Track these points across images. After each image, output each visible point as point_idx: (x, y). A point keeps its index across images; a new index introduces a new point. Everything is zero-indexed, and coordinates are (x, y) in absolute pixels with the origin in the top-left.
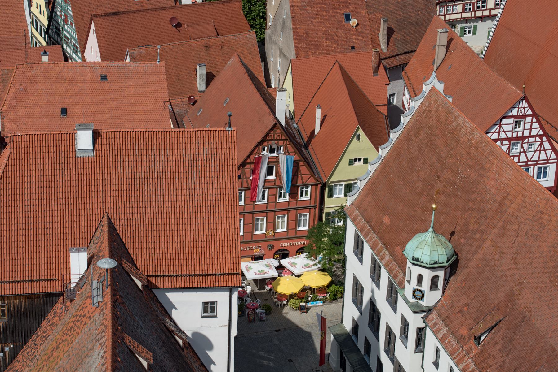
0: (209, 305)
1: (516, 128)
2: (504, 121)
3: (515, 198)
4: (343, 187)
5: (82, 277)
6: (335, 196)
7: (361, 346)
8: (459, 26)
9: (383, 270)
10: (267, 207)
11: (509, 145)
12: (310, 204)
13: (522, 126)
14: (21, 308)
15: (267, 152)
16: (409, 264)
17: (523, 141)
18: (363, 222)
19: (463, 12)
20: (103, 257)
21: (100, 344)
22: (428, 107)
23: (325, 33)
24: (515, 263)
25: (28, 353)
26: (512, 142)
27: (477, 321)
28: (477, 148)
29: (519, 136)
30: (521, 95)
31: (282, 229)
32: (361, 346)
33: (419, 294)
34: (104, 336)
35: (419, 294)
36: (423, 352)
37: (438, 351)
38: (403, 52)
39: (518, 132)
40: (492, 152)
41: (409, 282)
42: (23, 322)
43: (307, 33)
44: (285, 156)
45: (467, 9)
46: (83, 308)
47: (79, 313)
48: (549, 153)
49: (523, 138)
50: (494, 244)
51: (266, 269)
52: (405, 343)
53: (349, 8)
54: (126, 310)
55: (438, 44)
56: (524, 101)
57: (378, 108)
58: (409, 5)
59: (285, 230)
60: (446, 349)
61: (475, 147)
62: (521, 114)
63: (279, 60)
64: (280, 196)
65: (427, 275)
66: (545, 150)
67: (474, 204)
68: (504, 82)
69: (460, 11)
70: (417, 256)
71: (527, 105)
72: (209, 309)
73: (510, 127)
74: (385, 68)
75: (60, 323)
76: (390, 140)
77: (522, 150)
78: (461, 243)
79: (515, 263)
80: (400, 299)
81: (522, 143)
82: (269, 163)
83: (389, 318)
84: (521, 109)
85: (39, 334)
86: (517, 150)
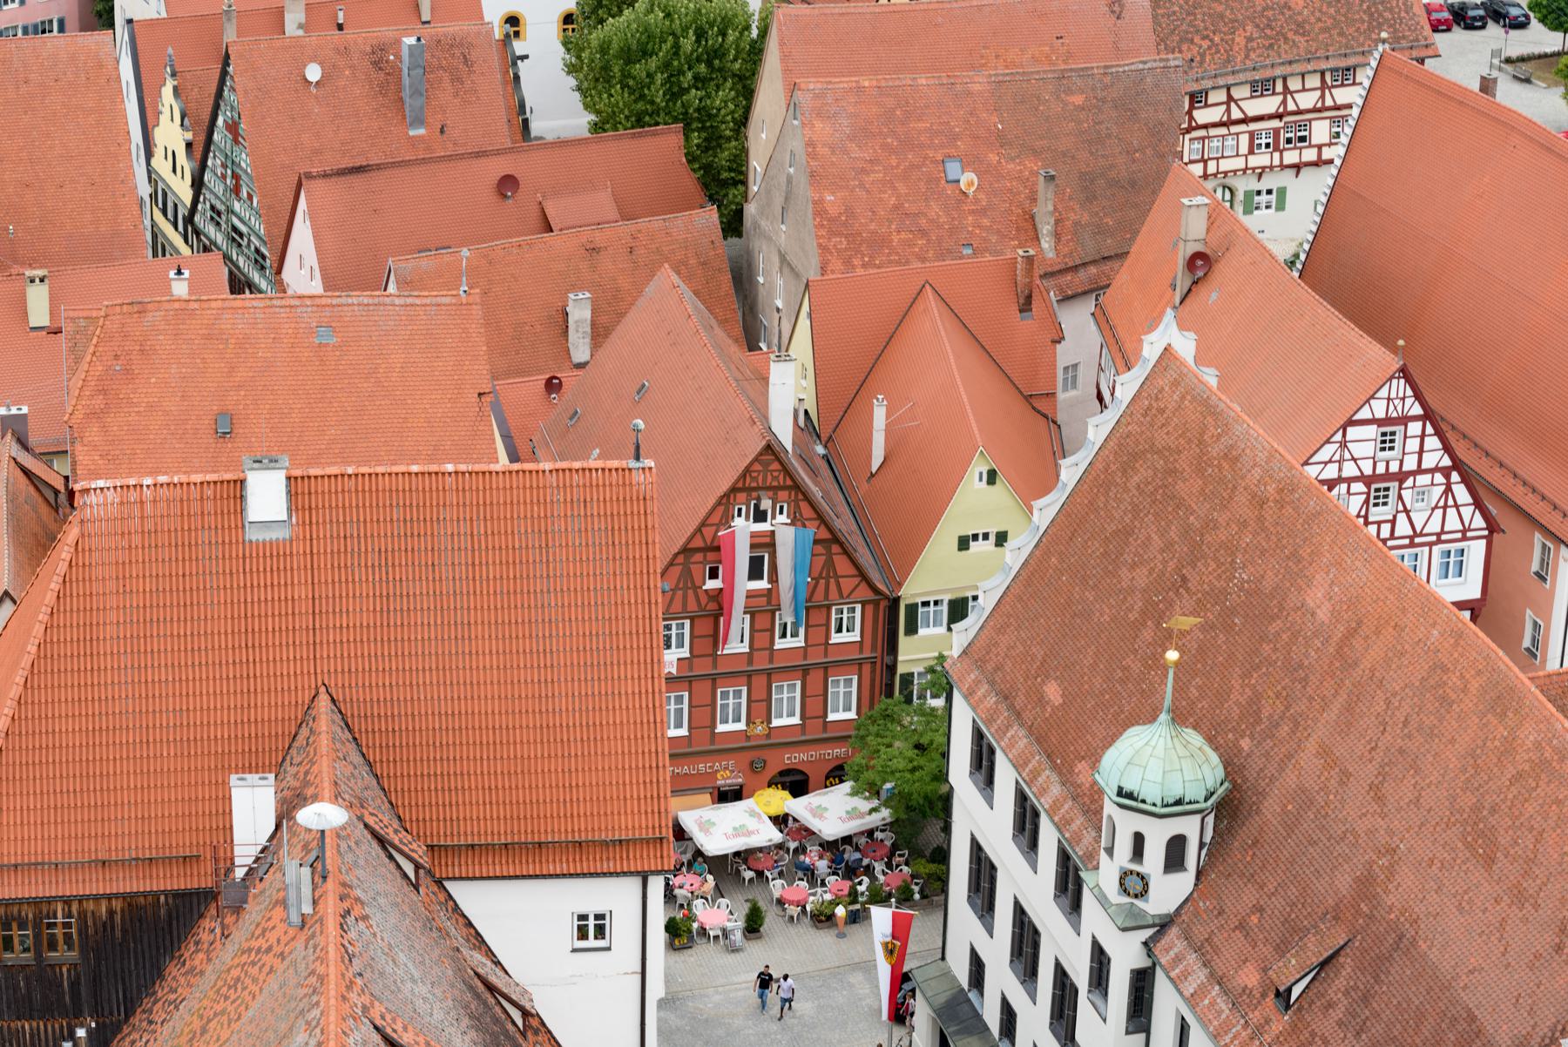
0: (591, 923)
1: (1383, 449)
2: (1353, 432)
3: (1378, 633)
4: (945, 608)
5: (262, 851)
6: (922, 631)
7: (992, 1017)
9: (1044, 822)
10: (750, 662)
11: (1368, 494)
12: (861, 651)
14: (113, 928)
15: (747, 518)
16: (1109, 809)
17: (1401, 482)
18: (992, 700)
19: (1251, 152)
20: (315, 798)
21: (308, 1023)
23: (896, 207)
24: (1379, 799)
25: (133, 1042)
26: (1374, 487)
27: (1282, 949)
28: (1281, 504)
31: (786, 720)
32: (992, 1017)
33: (1134, 884)
34: (317, 1004)
35: (1134, 884)
36: (1146, 1030)
37: (1184, 1029)
41: (1110, 851)
42: (118, 965)
43: (850, 212)
44: (792, 529)
46: (264, 931)
47: (255, 944)
48: (1467, 512)
49: (1401, 477)
50: (1324, 751)
51: (752, 824)
52: (1102, 1010)
53: (957, 147)
54: (375, 935)
58: (1109, 136)
59: (796, 720)
60: (1204, 1024)
63: (780, 282)
64: (784, 635)
65: (1157, 837)
66: (1456, 506)
67: (1275, 650)
69: (1244, 149)
70: (1128, 786)
71: (1409, 392)
72: (592, 928)
75: (210, 968)
77: (1401, 507)
78: (1240, 750)
79: (1379, 799)
80: (1088, 899)
81: (1400, 488)
82: (753, 546)
83: (1064, 947)
85: (160, 994)
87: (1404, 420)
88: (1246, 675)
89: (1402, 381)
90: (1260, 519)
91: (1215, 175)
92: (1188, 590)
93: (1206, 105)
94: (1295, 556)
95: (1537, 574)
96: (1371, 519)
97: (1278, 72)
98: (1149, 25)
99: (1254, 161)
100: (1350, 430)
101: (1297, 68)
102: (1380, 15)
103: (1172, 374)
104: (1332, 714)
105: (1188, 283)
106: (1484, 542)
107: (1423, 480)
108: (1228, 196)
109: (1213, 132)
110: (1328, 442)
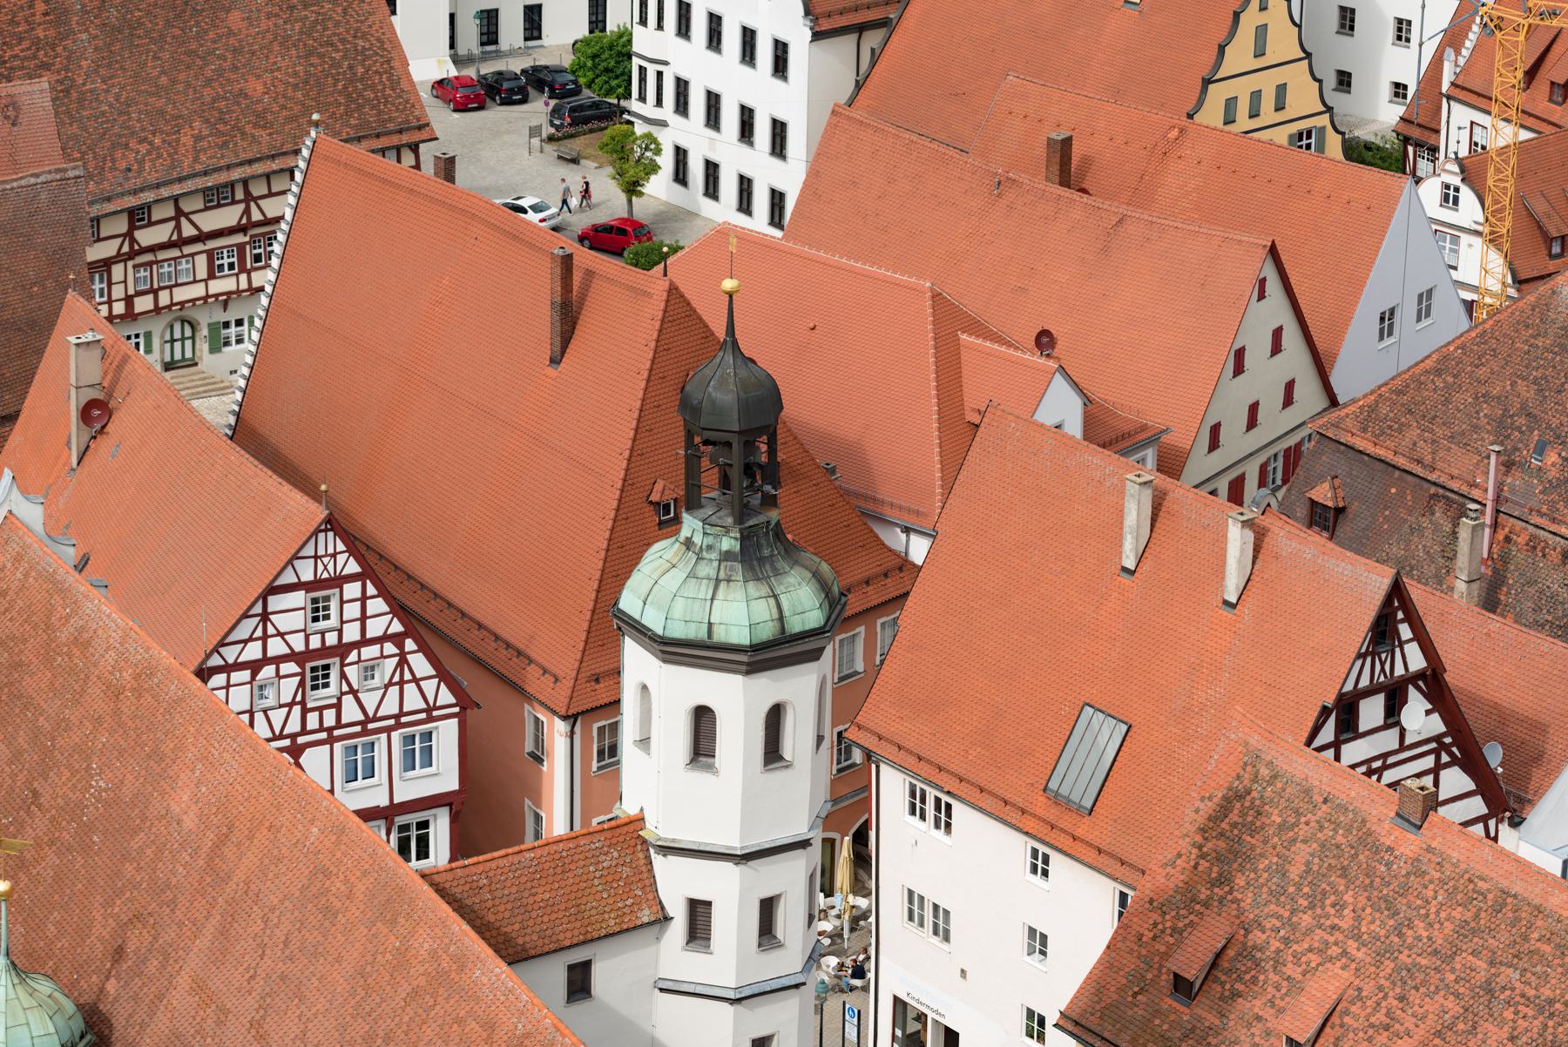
1: (316, 619)
2: (275, 602)
3: (251, 838)
11: (302, 674)
17: (343, 657)
19: (211, 276)
26: (309, 665)
28: (138, 692)
29: (312, 647)
30: (321, 513)
39: (323, 633)
45: (221, 267)
48: (429, 687)
49: (342, 650)
50: (199, 987)
61: (133, 690)
62: (325, 575)
66: (416, 680)
69: (202, 272)
71: (341, 547)
73: (296, 620)
77: (345, 688)
81: (343, 665)
84: (326, 560)
87: (339, 581)
88: (109, 903)
89: (331, 534)
90: (117, 712)
91: (169, 307)
92: (39, 807)
93: (151, 224)
95: (531, 754)
97: (236, 174)
98: (52, 129)
99: (217, 286)
100: (271, 599)
101: (259, 168)
102: (360, 95)
104: (203, 942)
105: (86, 437)
106: (455, 721)
107: (370, 652)
108: (188, 333)
109: (162, 255)
110: (246, 616)
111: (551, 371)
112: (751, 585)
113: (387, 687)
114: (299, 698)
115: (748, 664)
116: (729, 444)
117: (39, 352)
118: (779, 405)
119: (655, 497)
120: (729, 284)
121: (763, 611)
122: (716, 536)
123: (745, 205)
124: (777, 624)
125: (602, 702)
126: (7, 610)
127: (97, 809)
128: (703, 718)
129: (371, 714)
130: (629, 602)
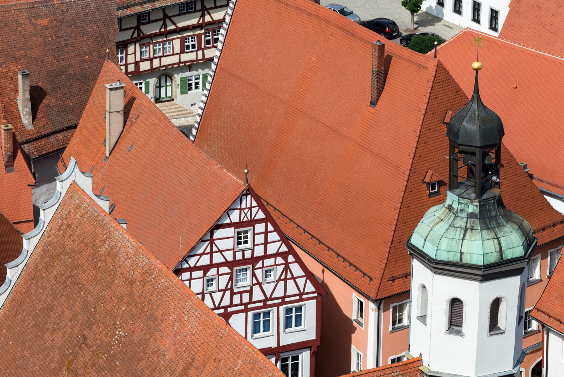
1: (239, 243)
2: (218, 234)
8: (177, 78)
11: (232, 274)
13: (250, 240)
19: (182, 51)
22: (67, 218)
26: (235, 269)
28: (144, 283)
29: (237, 259)
30: (244, 187)
38: (62, 127)
40: (167, 287)
45: (188, 47)
48: (301, 282)
49: (254, 260)
55: (108, 109)
56: (249, 197)
57: (16, 226)
58: (66, 45)
61: (140, 281)
62: (246, 219)
66: (294, 278)
68: (217, 167)
69: (177, 50)
71: (254, 204)
73: (229, 244)
74: (27, 158)
76: (7, 280)
77: (255, 282)
81: (254, 269)
84: (246, 211)
86: (245, 281)
87: (253, 222)
90: (131, 293)
93: (150, 22)
94: (153, 317)
96: (235, 291)
103: (76, 200)
107: (269, 262)
111: (371, 109)
112: (484, 232)
113: (278, 281)
114: (229, 287)
115: (482, 276)
116: (474, 154)
117: (89, 92)
118: (501, 133)
119: (427, 180)
120: (476, 65)
121: (491, 246)
122: (466, 204)
123: (476, 19)
124: (498, 254)
125: (395, 293)
126: (71, 235)
127: (119, 347)
128: (456, 304)
129: (268, 296)
130: (416, 240)
